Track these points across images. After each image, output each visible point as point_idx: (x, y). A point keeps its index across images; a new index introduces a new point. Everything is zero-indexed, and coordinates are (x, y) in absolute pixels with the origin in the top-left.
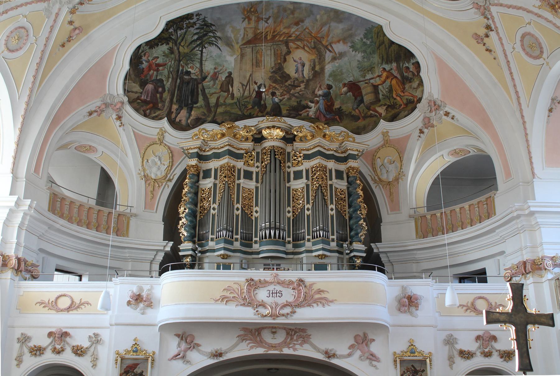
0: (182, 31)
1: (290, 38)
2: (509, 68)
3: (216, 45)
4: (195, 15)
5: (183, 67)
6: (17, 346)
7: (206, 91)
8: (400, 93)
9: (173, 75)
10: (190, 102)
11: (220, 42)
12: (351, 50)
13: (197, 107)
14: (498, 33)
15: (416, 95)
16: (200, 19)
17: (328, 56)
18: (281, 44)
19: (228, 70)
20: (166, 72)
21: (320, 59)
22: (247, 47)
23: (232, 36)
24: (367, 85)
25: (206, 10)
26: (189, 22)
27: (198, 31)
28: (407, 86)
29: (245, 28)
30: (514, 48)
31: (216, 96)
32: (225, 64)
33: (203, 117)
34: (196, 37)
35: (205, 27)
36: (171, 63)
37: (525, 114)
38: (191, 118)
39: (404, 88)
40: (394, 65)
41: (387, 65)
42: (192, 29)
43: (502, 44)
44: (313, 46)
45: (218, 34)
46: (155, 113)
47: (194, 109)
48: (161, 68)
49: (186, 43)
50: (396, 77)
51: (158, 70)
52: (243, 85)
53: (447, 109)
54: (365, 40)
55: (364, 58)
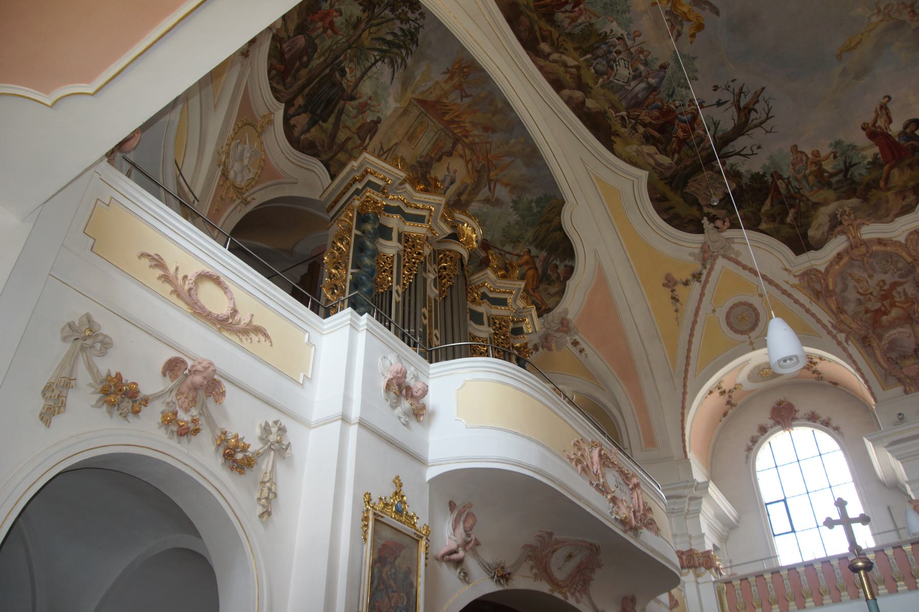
0: (390, 13)
1: (464, 139)
2: (692, 329)
3: (394, 70)
4: (420, 11)
5: (345, 59)
6: (62, 349)
7: (343, 116)
8: (530, 290)
9: (329, 55)
10: (318, 112)
11: (401, 71)
12: (511, 204)
13: (321, 126)
14: (704, 288)
15: (548, 302)
16: (418, 22)
17: (484, 193)
18: (450, 137)
19: (379, 115)
20: (328, 42)
21: (474, 189)
22: (416, 106)
23: (418, 78)
24: (500, 256)
25: (435, 19)
26: (406, 14)
27: (399, 33)
28: (542, 287)
29: (437, 82)
30: (714, 311)
31: (348, 134)
32: (383, 102)
33: (319, 148)
34: (390, 38)
35: (409, 37)
36: (341, 38)
37: (688, 383)
38: (308, 135)
39: (537, 287)
40: (544, 254)
41: (535, 249)
42: (398, 22)
43: (700, 301)
44: (478, 169)
45: (409, 61)
46: (278, 83)
47: (317, 126)
48: (330, 32)
49: (375, 33)
50: (536, 269)
51: (325, 31)
52: (382, 148)
53: (576, 337)
54: (533, 205)
55: (517, 224)
